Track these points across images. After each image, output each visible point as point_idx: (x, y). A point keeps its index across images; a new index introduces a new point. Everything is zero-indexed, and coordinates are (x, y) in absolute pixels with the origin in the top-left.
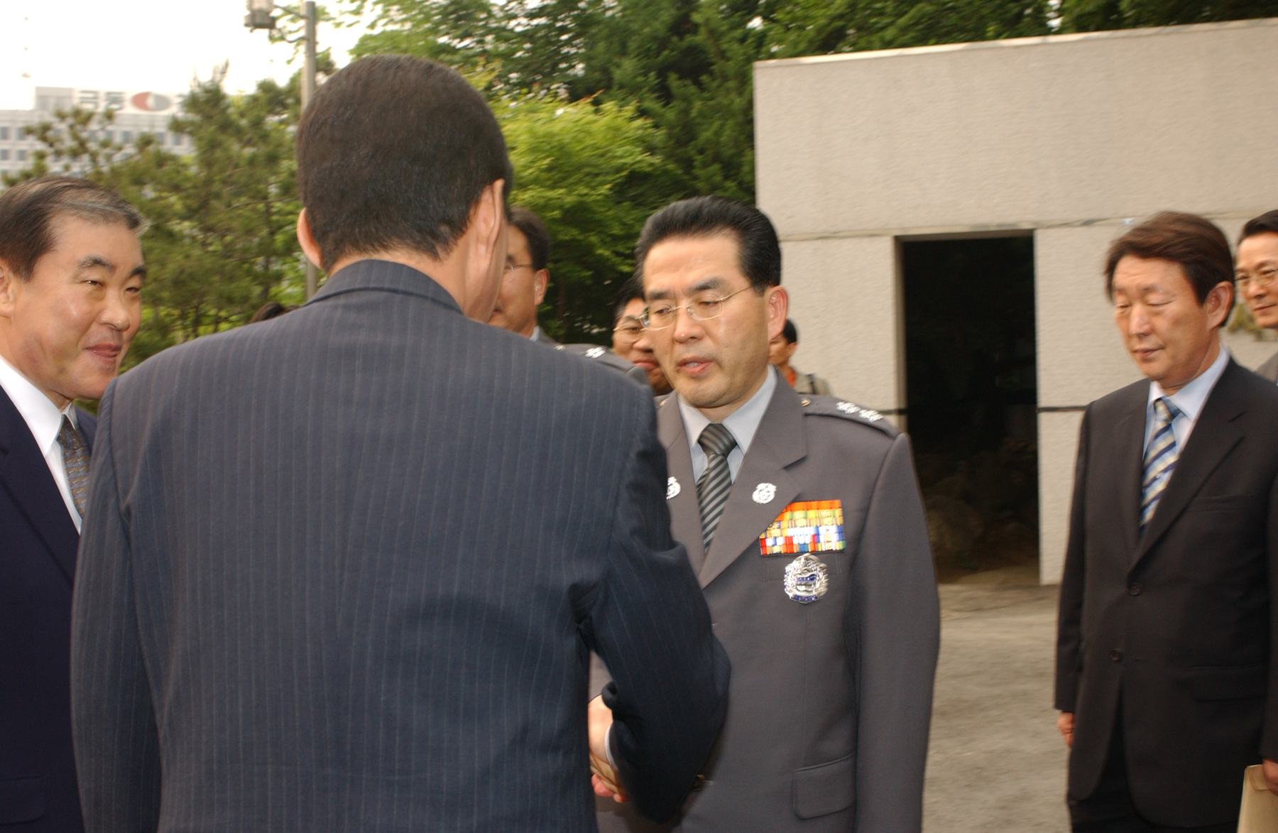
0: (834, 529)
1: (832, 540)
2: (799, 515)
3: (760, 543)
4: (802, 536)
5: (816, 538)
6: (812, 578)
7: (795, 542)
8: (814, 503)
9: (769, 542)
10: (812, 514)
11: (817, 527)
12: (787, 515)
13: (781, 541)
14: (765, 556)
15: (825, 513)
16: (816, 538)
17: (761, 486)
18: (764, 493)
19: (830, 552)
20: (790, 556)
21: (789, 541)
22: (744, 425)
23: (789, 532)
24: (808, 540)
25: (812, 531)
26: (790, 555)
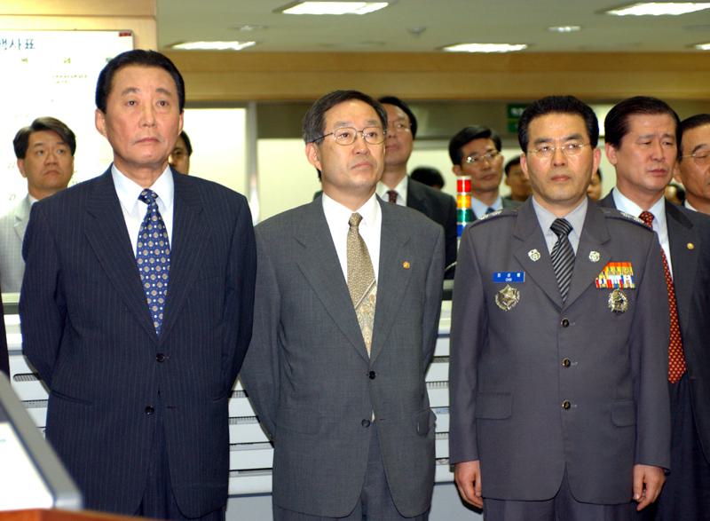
0: (629, 277)
1: (629, 282)
2: (613, 269)
3: (594, 283)
4: (615, 279)
5: (622, 281)
6: (622, 301)
8: (619, 263)
9: (600, 282)
11: (619, 276)
12: (607, 269)
13: (605, 282)
14: (599, 288)
15: (625, 269)
16: (622, 281)
17: (592, 253)
18: (594, 256)
19: (629, 288)
21: (609, 282)
22: (577, 217)
23: (610, 277)
25: (619, 278)
26: (610, 288)
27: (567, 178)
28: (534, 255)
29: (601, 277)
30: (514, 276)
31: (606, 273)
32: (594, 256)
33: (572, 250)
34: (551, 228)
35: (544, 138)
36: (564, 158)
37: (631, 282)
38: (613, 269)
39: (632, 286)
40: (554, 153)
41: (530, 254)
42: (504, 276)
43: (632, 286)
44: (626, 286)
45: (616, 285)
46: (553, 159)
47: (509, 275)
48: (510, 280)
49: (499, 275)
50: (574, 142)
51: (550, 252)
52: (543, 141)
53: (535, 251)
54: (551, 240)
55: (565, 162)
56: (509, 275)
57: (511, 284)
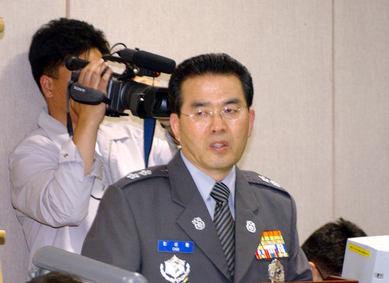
0: (282, 247)
5: (276, 250)
6: (279, 273)
7: (270, 252)
8: (271, 232)
10: (272, 237)
12: (263, 239)
15: (277, 237)
19: (284, 258)
20: (269, 260)
23: (266, 247)
24: (275, 252)
26: (269, 260)
27: (225, 144)
28: (199, 224)
29: (260, 247)
30: (181, 246)
31: (262, 243)
32: (251, 226)
33: (232, 216)
34: (212, 194)
35: (202, 102)
36: (225, 124)
37: (284, 251)
38: (267, 238)
39: (286, 255)
40: (213, 117)
41: (194, 222)
42: (171, 245)
43: (286, 255)
44: (281, 255)
45: (273, 255)
46: (212, 125)
47: (176, 244)
48: (178, 249)
49: (165, 244)
50: (231, 106)
51: (213, 218)
52: (201, 105)
53: (199, 219)
54: (211, 206)
55: (225, 127)
56: (176, 244)
57: (180, 256)
